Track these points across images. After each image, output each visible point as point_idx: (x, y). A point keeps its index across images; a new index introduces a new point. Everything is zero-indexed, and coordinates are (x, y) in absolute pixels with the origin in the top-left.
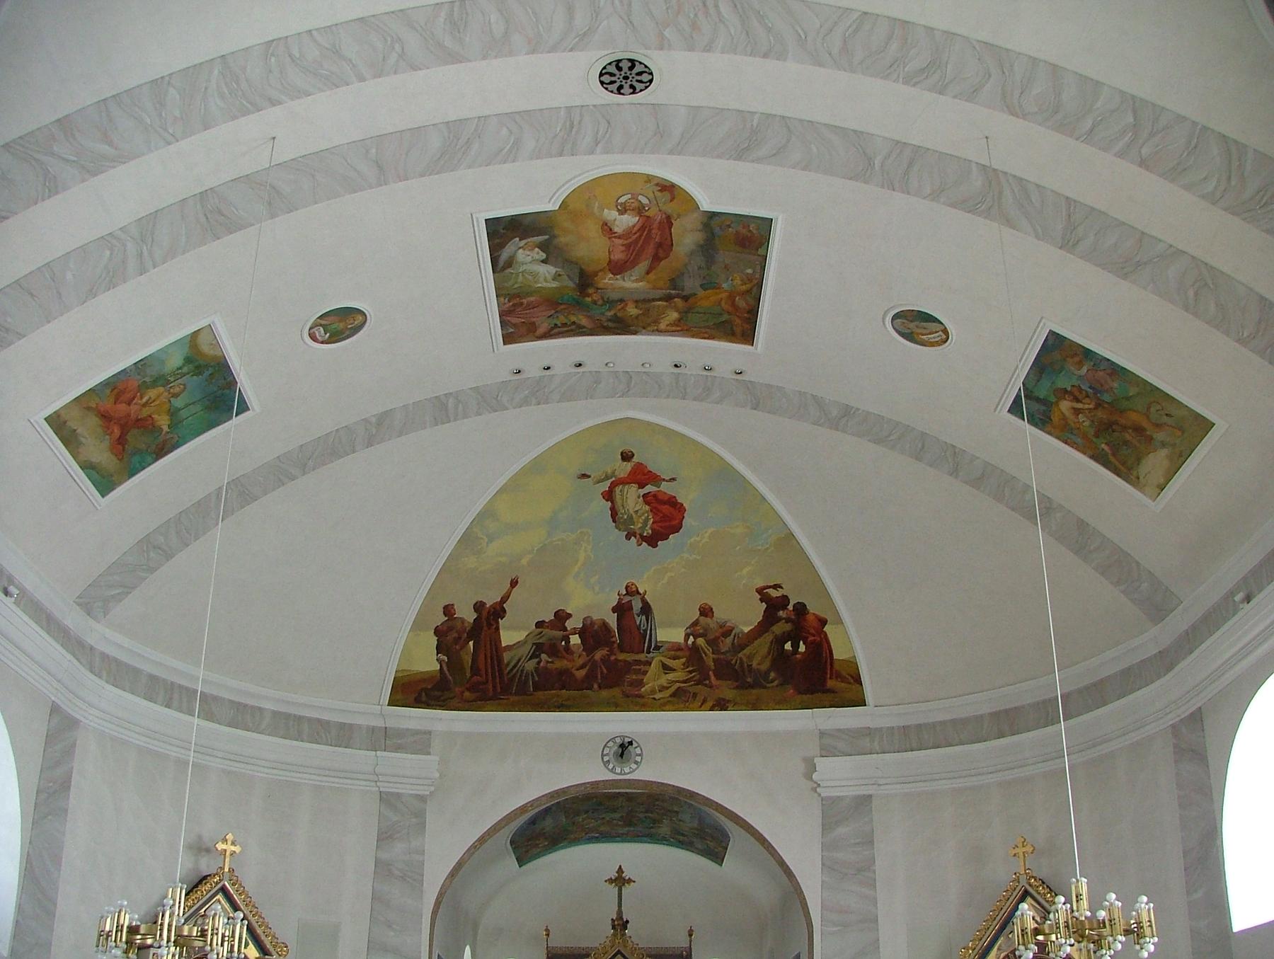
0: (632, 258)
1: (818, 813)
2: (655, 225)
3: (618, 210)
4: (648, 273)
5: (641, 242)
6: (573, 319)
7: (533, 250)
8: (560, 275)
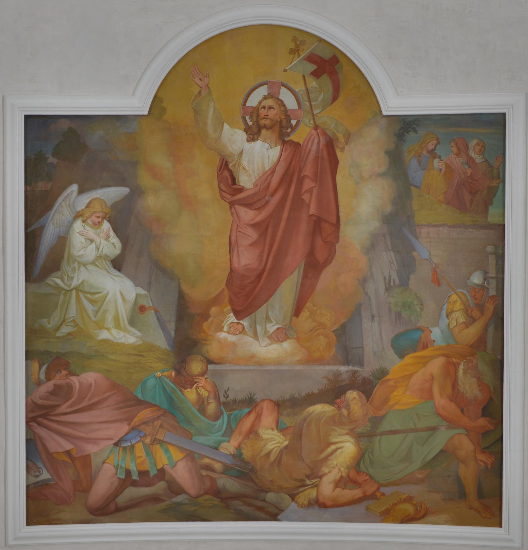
0: (268, 266)
2: (308, 171)
4: (297, 312)
5: (285, 214)
7: (100, 223)
8: (142, 309)
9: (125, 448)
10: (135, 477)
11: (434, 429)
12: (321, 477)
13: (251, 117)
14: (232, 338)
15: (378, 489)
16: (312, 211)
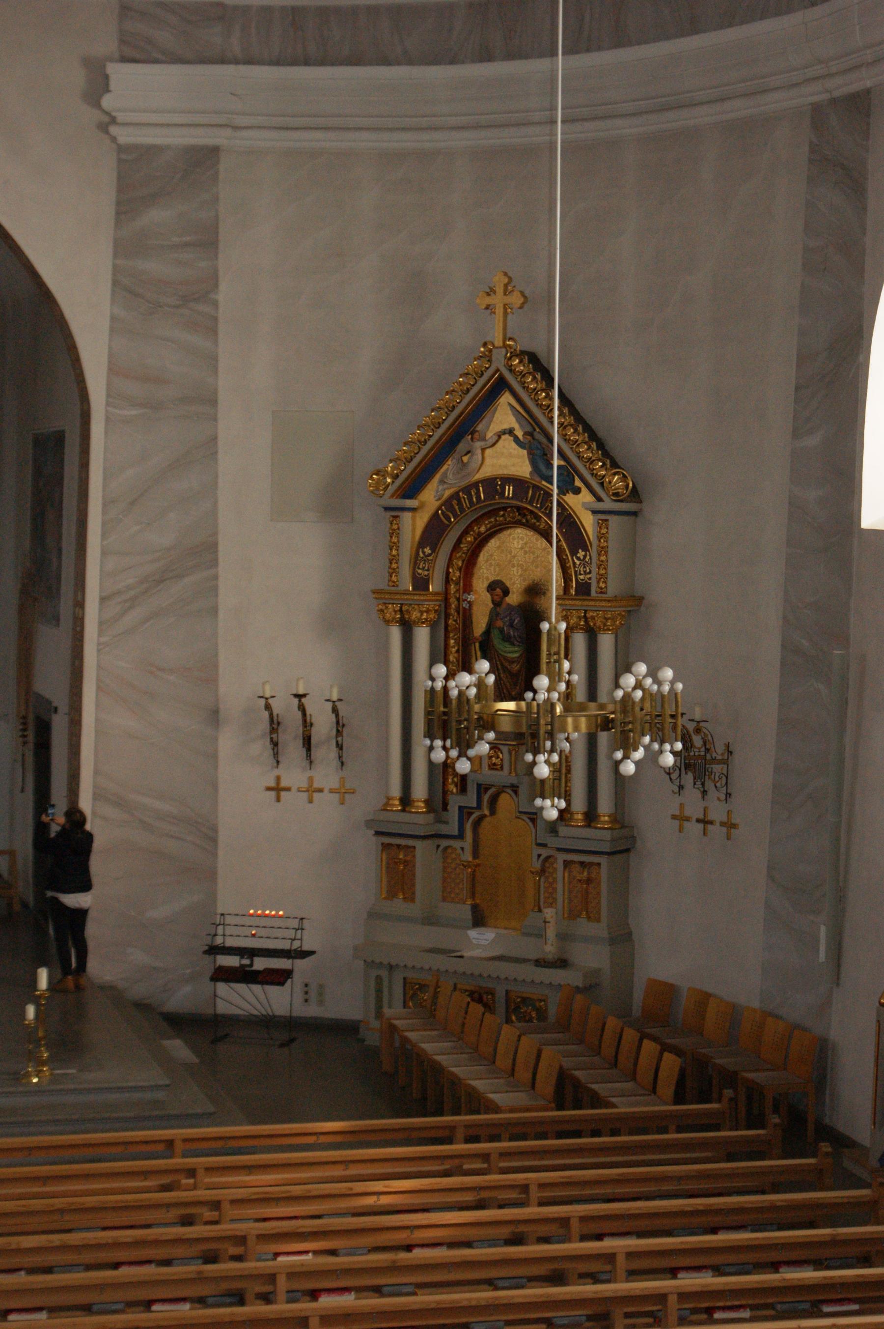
1: (108, 177)
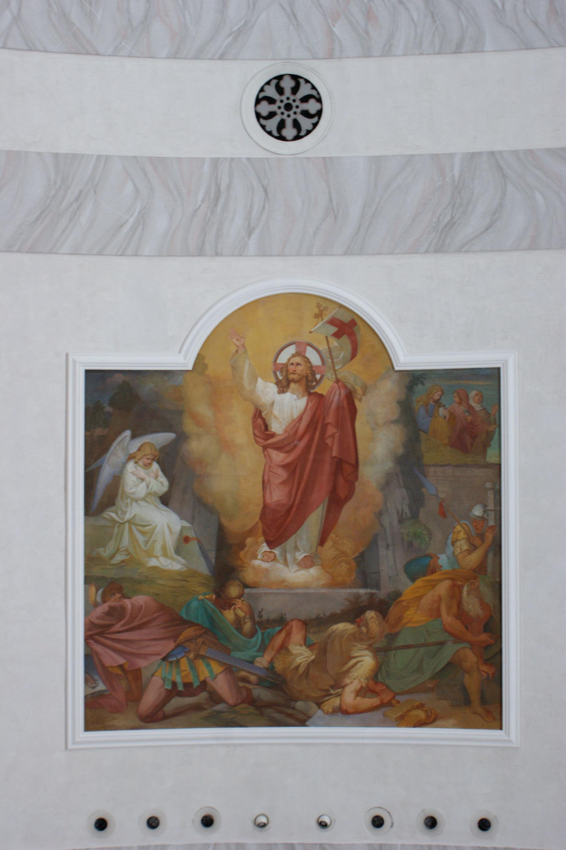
0: (297, 502)
2: (330, 419)
3: (278, 383)
4: (322, 542)
5: (311, 456)
6: (204, 672)
7: (150, 464)
8: (187, 540)
9: (171, 662)
10: (180, 688)
11: (442, 644)
12: (343, 687)
13: (281, 372)
14: (265, 565)
15: (394, 697)
16: (334, 454)
